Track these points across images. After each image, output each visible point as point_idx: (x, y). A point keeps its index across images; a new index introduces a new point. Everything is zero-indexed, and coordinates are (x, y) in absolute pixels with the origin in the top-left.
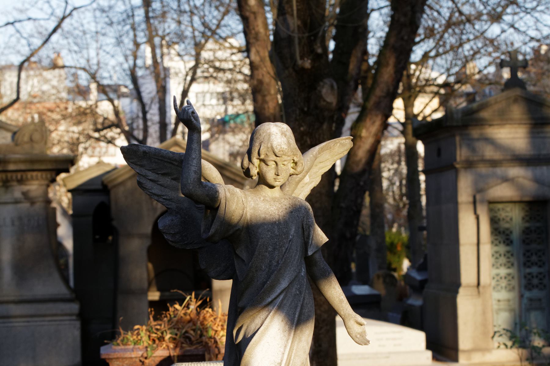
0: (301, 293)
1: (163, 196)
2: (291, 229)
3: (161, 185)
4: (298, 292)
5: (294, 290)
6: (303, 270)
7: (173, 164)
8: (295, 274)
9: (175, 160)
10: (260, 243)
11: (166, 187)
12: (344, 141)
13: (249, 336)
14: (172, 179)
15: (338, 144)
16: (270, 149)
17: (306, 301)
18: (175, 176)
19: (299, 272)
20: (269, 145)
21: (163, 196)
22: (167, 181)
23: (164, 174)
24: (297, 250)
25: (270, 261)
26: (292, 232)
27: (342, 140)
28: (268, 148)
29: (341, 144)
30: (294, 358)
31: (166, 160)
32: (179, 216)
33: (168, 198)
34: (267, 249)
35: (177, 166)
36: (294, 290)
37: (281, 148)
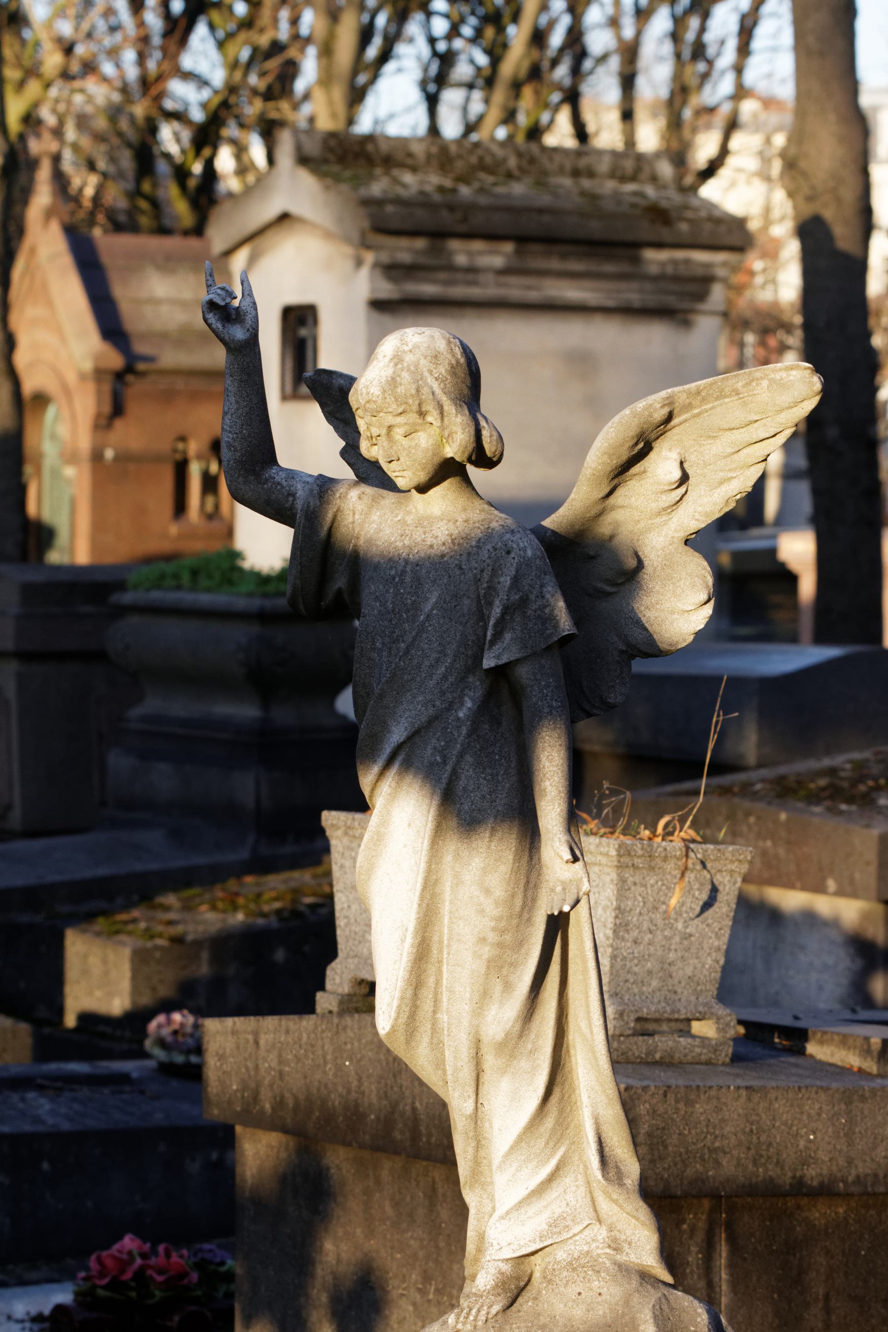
0: (445, 762)
2: (427, 599)
4: (438, 758)
5: (429, 751)
6: (469, 704)
8: (431, 711)
12: (784, 374)
15: (765, 383)
17: (462, 783)
19: (450, 707)
24: (443, 652)
26: (427, 607)
27: (773, 371)
29: (772, 381)
30: (451, 922)
34: (374, 643)
36: (429, 751)
37: (368, 393)
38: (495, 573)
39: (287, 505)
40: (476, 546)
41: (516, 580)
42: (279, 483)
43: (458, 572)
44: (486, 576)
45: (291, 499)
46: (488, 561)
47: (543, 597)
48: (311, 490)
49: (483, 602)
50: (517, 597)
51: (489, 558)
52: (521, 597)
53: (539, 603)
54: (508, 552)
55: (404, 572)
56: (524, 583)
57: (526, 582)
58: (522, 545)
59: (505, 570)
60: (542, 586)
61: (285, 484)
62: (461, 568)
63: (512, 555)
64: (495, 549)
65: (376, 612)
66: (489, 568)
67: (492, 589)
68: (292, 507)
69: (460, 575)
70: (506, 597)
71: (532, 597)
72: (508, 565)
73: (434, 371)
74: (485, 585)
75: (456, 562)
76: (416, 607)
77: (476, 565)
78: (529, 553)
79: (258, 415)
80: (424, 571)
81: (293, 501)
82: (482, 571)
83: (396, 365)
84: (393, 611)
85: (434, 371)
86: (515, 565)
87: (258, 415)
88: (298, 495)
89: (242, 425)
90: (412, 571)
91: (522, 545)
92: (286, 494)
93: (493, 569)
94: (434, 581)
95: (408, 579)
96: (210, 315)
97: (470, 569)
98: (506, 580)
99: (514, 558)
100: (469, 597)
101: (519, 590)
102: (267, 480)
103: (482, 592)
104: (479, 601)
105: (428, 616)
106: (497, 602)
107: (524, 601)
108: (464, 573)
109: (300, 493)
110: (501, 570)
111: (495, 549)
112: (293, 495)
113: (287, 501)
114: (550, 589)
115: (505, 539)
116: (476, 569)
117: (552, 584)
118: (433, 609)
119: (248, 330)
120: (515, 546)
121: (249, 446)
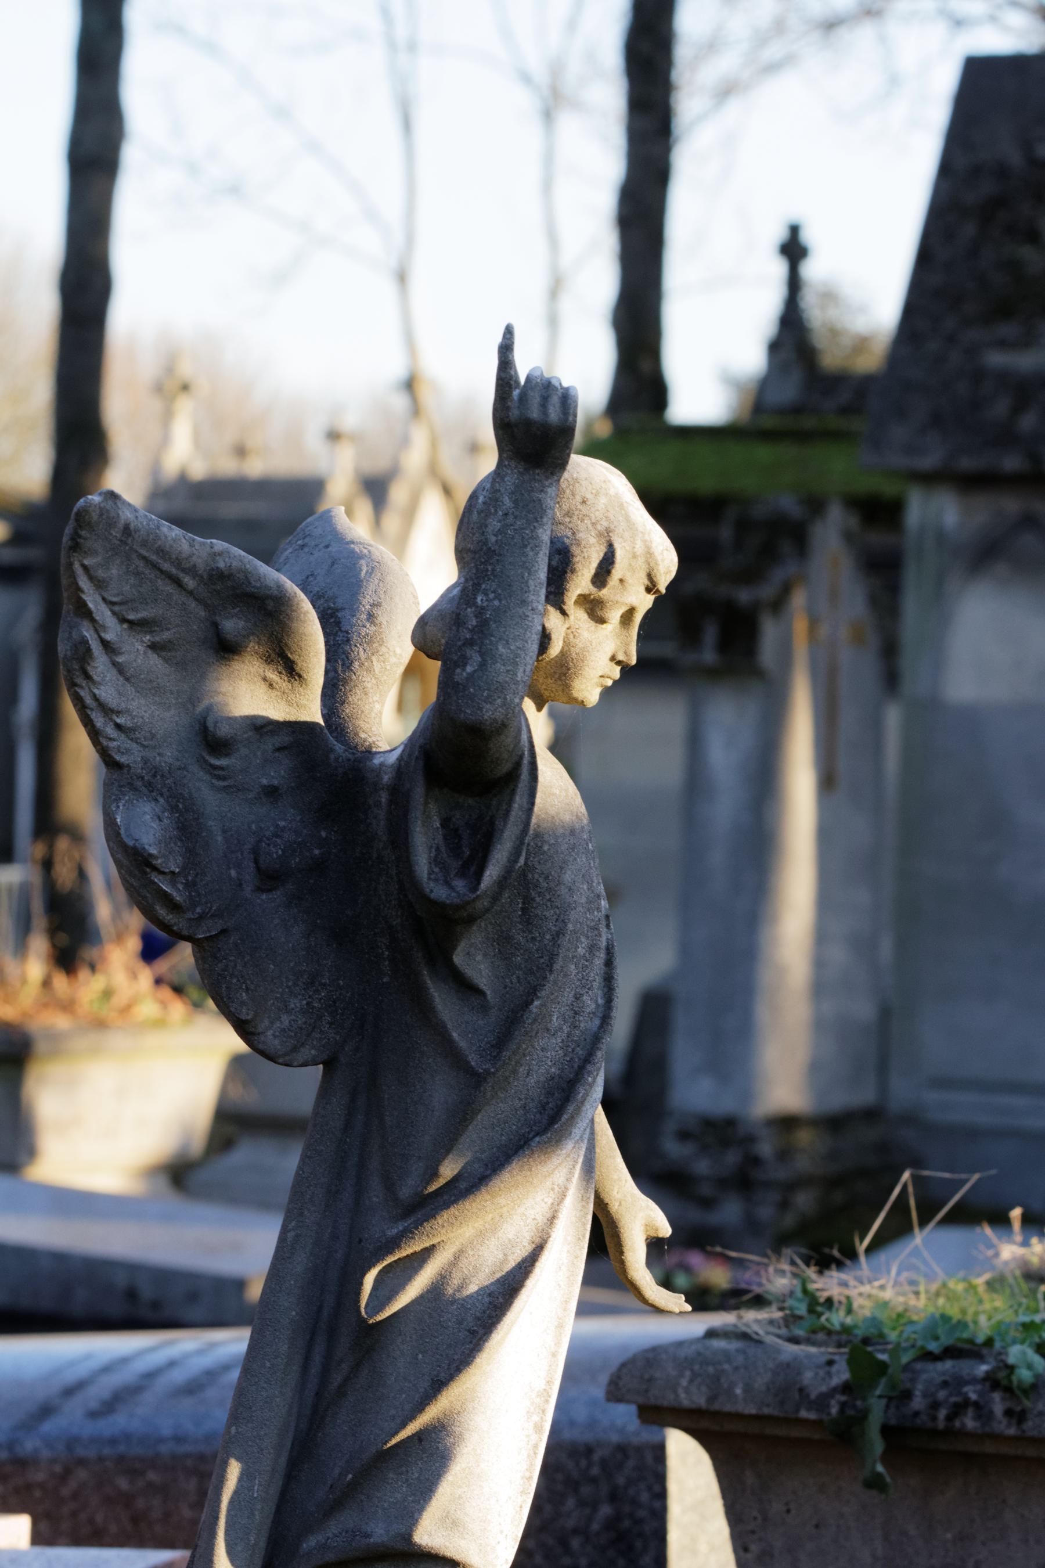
1: (118, 713)
3: (120, 669)
7: (178, 583)
9: (192, 571)
10: (570, 926)
11: (127, 679)
13: (473, 1288)
14: (153, 647)
16: (641, 561)
18: (166, 635)
20: (639, 548)
21: (118, 713)
22: (135, 650)
23: (133, 625)
25: (578, 997)
28: (635, 556)
31: (166, 566)
32: (162, 800)
33: (129, 724)
35: (191, 593)
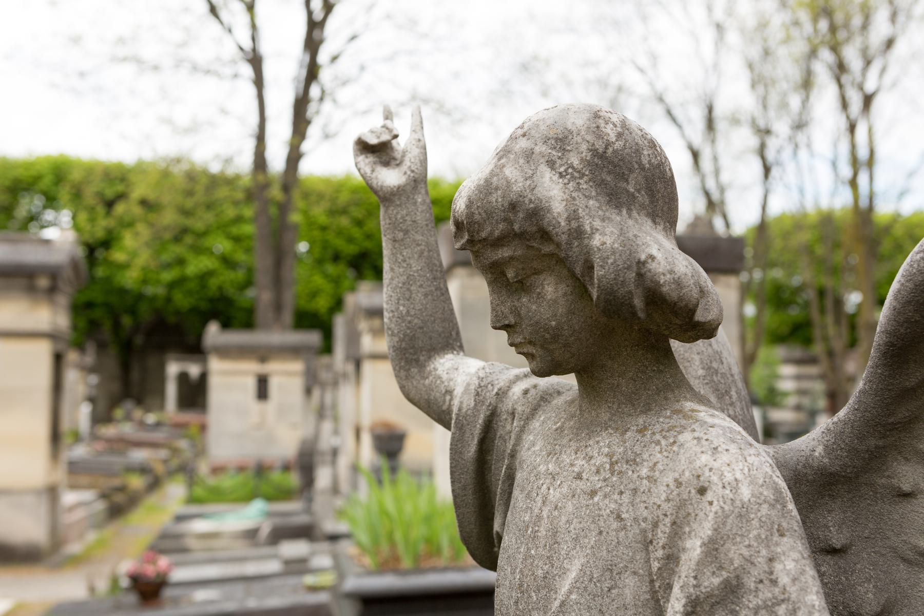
2: (565, 571)
38: (677, 531)
39: (445, 407)
40: (648, 478)
41: (713, 550)
42: (440, 378)
43: (615, 525)
44: (661, 537)
45: (448, 398)
46: (665, 506)
47: (774, 582)
48: (468, 385)
49: (657, 584)
50: (716, 581)
51: (668, 500)
52: (726, 583)
53: (766, 593)
54: (702, 491)
55: (539, 517)
56: (731, 555)
57: (735, 553)
58: (729, 477)
59: (695, 526)
60: (771, 560)
61: (445, 377)
62: (619, 518)
63: (709, 496)
64: (679, 484)
65: (507, 583)
66: (668, 521)
67: (672, 559)
68: (449, 412)
69: (617, 531)
70: (693, 581)
71: (750, 583)
72: (701, 515)
73: (559, 162)
74: (660, 553)
75: (613, 506)
76: (547, 584)
77: (645, 513)
78: (746, 493)
79: (421, 286)
80: (564, 519)
81: (451, 400)
82: (655, 525)
83: (499, 159)
84: (521, 586)
85: (559, 162)
86: (711, 515)
87: (421, 286)
88: (455, 393)
89: (399, 299)
90: (548, 517)
91: (729, 477)
92: (444, 391)
93: (674, 523)
94: (576, 539)
95: (542, 532)
96: (361, 158)
97: (636, 520)
98: (693, 548)
99: (711, 503)
100: (635, 573)
101: (721, 568)
102: (430, 372)
103: (656, 565)
104: (652, 581)
105: (563, 604)
106: (676, 590)
107: (732, 590)
108: (624, 528)
109: (458, 391)
110: (689, 524)
111: (679, 484)
112: (449, 392)
113: (444, 401)
114: (790, 565)
115: (698, 464)
116: (645, 520)
117: (796, 555)
118: (570, 592)
119: (405, 173)
120: (715, 479)
121: (408, 328)
